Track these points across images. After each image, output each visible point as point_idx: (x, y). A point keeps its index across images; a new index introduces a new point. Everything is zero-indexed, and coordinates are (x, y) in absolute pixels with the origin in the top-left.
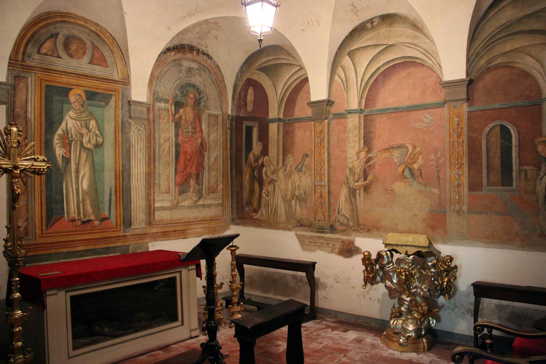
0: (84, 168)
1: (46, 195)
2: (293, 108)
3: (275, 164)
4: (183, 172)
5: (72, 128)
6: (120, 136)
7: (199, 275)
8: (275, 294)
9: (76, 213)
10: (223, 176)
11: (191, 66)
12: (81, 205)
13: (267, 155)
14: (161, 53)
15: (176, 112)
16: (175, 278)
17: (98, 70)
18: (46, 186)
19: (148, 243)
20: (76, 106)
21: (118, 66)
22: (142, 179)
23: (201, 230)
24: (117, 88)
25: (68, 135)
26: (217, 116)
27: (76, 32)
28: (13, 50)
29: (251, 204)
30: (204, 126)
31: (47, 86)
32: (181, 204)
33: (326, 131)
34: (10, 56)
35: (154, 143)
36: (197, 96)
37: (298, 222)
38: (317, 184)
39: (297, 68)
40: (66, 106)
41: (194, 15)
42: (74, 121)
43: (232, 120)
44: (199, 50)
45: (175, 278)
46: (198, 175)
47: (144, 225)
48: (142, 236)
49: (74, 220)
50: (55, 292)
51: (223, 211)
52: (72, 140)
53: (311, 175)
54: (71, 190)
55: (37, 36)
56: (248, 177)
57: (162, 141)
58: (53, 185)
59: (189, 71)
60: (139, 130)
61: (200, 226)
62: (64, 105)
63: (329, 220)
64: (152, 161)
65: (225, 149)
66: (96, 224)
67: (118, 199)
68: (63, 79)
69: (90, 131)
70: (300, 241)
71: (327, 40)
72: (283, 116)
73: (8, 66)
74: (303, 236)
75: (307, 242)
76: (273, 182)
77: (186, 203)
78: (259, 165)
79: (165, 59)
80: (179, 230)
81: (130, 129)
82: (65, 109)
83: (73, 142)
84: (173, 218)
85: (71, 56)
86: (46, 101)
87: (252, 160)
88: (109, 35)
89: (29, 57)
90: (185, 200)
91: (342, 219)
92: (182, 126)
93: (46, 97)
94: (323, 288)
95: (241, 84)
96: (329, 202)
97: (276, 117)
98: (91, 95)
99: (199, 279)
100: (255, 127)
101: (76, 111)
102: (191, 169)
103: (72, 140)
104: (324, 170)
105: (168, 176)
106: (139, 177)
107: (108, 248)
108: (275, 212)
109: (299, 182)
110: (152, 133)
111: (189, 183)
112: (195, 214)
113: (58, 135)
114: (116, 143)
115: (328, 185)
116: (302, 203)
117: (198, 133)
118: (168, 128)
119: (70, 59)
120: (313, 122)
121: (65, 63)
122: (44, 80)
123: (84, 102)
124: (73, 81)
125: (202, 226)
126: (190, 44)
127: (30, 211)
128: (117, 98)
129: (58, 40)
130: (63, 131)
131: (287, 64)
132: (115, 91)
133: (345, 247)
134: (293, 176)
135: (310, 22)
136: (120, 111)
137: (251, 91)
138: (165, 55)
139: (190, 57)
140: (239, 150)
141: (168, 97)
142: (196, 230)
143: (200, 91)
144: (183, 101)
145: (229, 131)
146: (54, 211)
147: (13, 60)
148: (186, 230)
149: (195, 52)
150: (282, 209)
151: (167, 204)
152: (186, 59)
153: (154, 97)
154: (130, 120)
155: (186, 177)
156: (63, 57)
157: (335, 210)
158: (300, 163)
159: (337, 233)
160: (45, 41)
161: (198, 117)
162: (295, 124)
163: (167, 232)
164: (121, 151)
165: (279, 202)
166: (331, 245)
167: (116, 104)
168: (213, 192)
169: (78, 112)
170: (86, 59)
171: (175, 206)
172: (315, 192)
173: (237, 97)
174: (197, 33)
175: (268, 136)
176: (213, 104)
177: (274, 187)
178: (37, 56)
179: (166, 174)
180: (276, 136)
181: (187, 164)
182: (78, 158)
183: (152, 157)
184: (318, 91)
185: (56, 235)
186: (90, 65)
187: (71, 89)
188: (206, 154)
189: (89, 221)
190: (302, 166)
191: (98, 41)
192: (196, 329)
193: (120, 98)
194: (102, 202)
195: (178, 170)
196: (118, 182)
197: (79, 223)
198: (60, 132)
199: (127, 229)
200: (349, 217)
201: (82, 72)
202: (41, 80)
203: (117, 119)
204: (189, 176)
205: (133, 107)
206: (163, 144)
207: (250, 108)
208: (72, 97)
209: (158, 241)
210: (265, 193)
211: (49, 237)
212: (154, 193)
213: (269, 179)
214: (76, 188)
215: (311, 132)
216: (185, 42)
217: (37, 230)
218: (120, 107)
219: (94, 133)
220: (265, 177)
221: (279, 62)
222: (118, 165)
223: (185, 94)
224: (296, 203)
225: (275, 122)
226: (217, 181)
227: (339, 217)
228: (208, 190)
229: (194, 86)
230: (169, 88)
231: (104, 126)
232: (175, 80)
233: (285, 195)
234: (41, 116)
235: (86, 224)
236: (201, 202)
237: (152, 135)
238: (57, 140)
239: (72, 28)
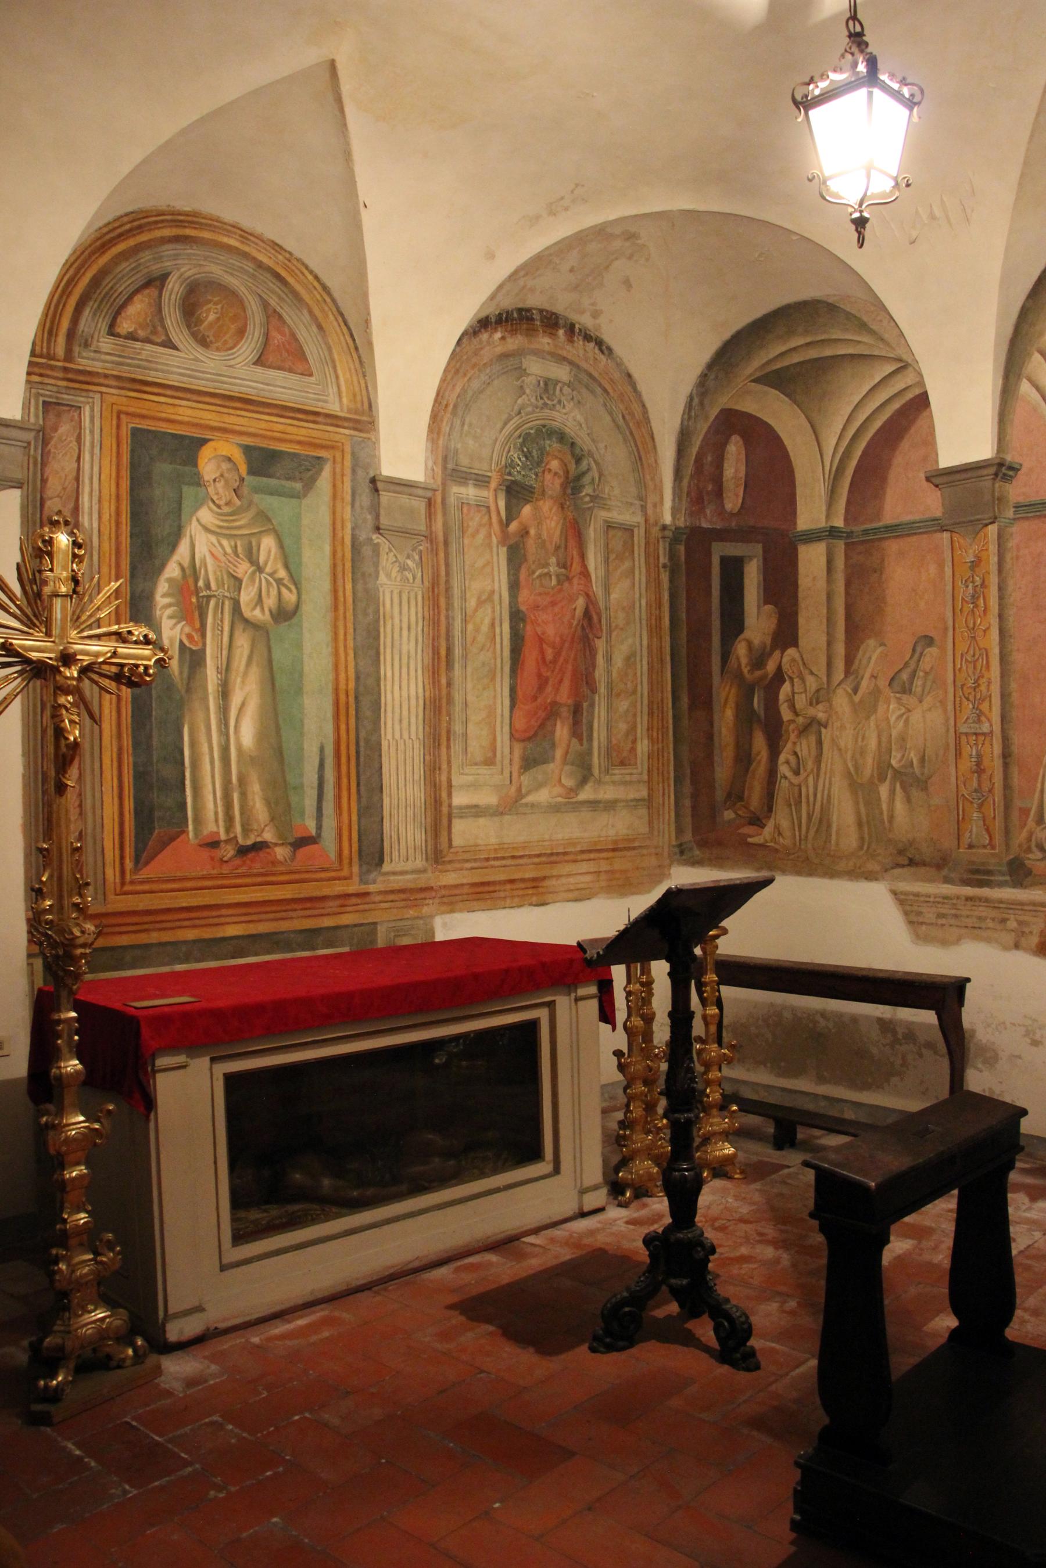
0: (243, 682)
1: (135, 764)
2: (879, 494)
3: (822, 673)
4: (535, 698)
5: (210, 561)
6: (349, 586)
7: (607, 1015)
8: (821, 1080)
9: (221, 823)
10: (651, 713)
11: (552, 376)
12: (236, 796)
13: (795, 643)
14: (465, 334)
15: (512, 514)
16: (532, 1026)
17: (280, 385)
18: (134, 737)
19: (432, 917)
20: (220, 491)
21: (340, 372)
22: (413, 720)
23: (588, 878)
24: (337, 437)
25: (196, 581)
26: (629, 530)
27: (215, 270)
28: (42, 324)
29: (741, 798)
30: (593, 561)
31: (135, 432)
32: (530, 799)
33: (994, 559)
34: (34, 344)
35: (449, 606)
36: (572, 466)
37: (901, 852)
38: (963, 729)
39: (889, 368)
40: (188, 491)
41: (566, 209)
42: (213, 539)
43: (675, 541)
44: (572, 327)
45: (532, 1026)
46: (577, 711)
47: (420, 863)
48: (414, 895)
49: (214, 844)
50: (181, 1059)
51: (650, 823)
52: (209, 597)
53: (943, 703)
54: (205, 748)
55: (107, 282)
56: (729, 713)
57: (472, 603)
58: (155, 733)
59: (546, 390)
60: (404, 568)
61: (584, 867)
62: (185, 489)
63: (1007, 845)
64: (443, 664)
65: (655, 630)
66: (280, 857)
67: (345, 781)
68: (181, 410)
69: (260, 569)
70: (906, 913)
71: (994, 270)
72: (846, 520)
73: (29, 374)
74: (917, 895)
75: (929, 915)
76: (814, 728)
77: (542, 796)
78: (766, 675)
79: (476, 353)
80: (523, 880)
81: (376, 565)
82: (186, 504)
83: (212, 603)
84: (506, 840)
85: (203, 342)
86: (132, 479)
87: (744, 661)
88: (310, 277)
89: (86, 345)
90: (539, 786)
92: (531, 558)
93: (134, 466)
94: (985, 1062)
95: (702, 428)
96: (1007, 786)
97: (822, 524)
98: (263, 461)
99: (609, 1027)
100: (751, 558)
101: (219, 507)
102: (557, 690)
103: (209, 597)
104: (989, 683)
105: (491, 711)
106: (405, 713)
107: (315, 932)
108: (824, 823)
109: (901, 724)
110: (443, 579)
111: (553, 732)
112: (572, 830)
113: (170, 580)
114: (336, 608)
115: (1003, 730)
116: (915, 793)
117: (575, 581)
118: (488, 563)
119: (200, 349)
120: (946, 535)
121: (184, 362)
122: (127, 414)
123: (242, 480)
124: (209, 416)
125: (591, 867)
126: (546, 306)
127: (90, 814)
128: (338, 470)
129: (166, 295)
130: (183, 569)
131: (852, 357)
132: (333, 447)
134: (881, 708)
135: (937, 213)
136: (348, 509)
137: (735, 448)
138: (475, 341)
139: (547, 348)
140: (698, 632)
141: (485, 466)
142: (572, 880)
143: (577, 451)
144: (531, 480)
145: (665, 577)
146: (157, 814)
147: (41, 356)
148: (544, 878)
149: (561, 332)
150: (844, 813)
151: (488, 798)
152: (536, 353)
153: (445, 468)
154: (376, 538)
155: (542, 714)
156: (180, 346)
157: (1025, 812)
159: (1032, 885)
160: (129, 299)
161: (575, 531)
162: (886, 544)
163: (488, 883)
164: (351, 631)
165: (835, 789)
166: (1012, 924)
167: (334, 486)
168: (622, 763)
169: (226, 510)
170: (247, 349)
171: (512, 805)
172: (958, 753)
173: (689, 469)
174: (571, 270)
175: (795, 585)
176: (617, 492)
177: (820, 743)
178: (106, 344)
179: (485, 704)
180: (822, 583)
181: (546, 673)
182: (225, 653)
183: (443, 652)
184: (963, 431)
185: (164, 886)
186: (259, 369)
187: (204, 442)
188: (600, 645)
189: (260, 846)
190: (913, 675)
191: (280, 298)
192: (596, 1188)
193: (348, 471)
194: (295, 788)
195: (520, 693)
196: (343, 727)
197: (229, 852)
198: (172, 571)
199: (369, 872)
201: (235, 390)
202: (119, 413)
203: (340, 535)
204: (552, 712)
205: (386, 497)
206: (476, 610)
207: (733, 502)
208: (208, 466)
209: (461, 911)
210: (787, 762)
211: (145, 892)
212: (449, 762)
213: (800, 720)
214: (220, 745)
215: (941, 566)
216: (534, 301)
217: (109, 872)
218: (348, 498)
219: (271, 575)
220: (786, 714)
221: (828, 352)
222: (342, 676)
223: (536, 461)
224: (892, 792)
225: (819, 539)
226: (633, 728)
228: (608, 754)
229: (562, 437)
230: (487, 443)
231: (300, 555)
232: (504, 417)
233: (856, 768)
234: (118, 524)
235: (250, 856)
236: (586, 794)
237: (442, 586)
238: (163, 596)
239: (206, 258)
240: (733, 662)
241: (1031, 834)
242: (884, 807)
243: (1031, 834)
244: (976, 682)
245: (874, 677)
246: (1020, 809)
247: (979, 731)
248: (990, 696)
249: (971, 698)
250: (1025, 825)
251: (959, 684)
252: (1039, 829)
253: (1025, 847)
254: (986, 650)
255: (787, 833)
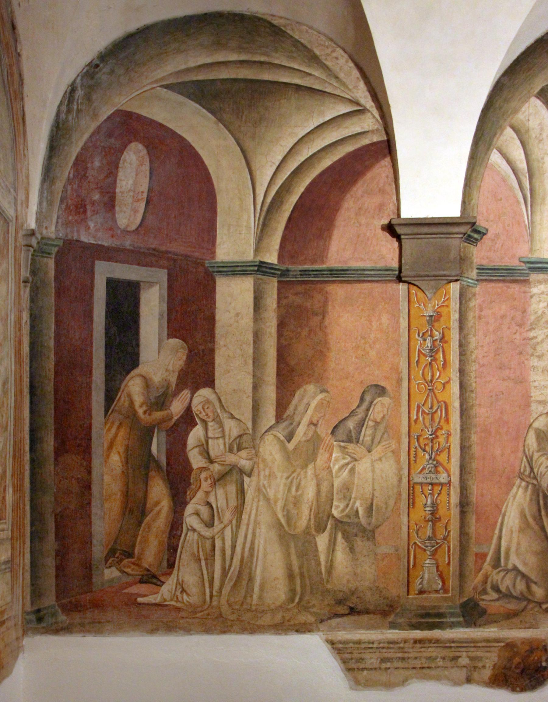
3: (247, 416)
37: (340, 602)
63: (461, 587)
70: (344, 662)
74: (359, 642)
75: (372, 660)
87: (138, 399)
91: (506, 583)
104: (449, 435)
109: (345, 474)
133: (517, 660)
158: (353, 413)
166: (464, 661)
172: (411, 503)
177: (241, 492)
190: (361, 424)
200: (533, 577)
210: (197, 514)
213: (216, 468)
220: (196, 460)
224: (332, 543)
227: (496, 576)
240: (122, 401)
241: (486, 577)
242: (322, 558)
243: (486, 577)
244: (434, 433)
245: (313, 424)
246: (476, 555)
247: (436, 481)
248: (449, 449)
249: (428, 449)
250: (481, 569)
251: (414, 435)
252: (495, 571)
253: (480, 589)
254: (445, 402)
255: (194, 590)
